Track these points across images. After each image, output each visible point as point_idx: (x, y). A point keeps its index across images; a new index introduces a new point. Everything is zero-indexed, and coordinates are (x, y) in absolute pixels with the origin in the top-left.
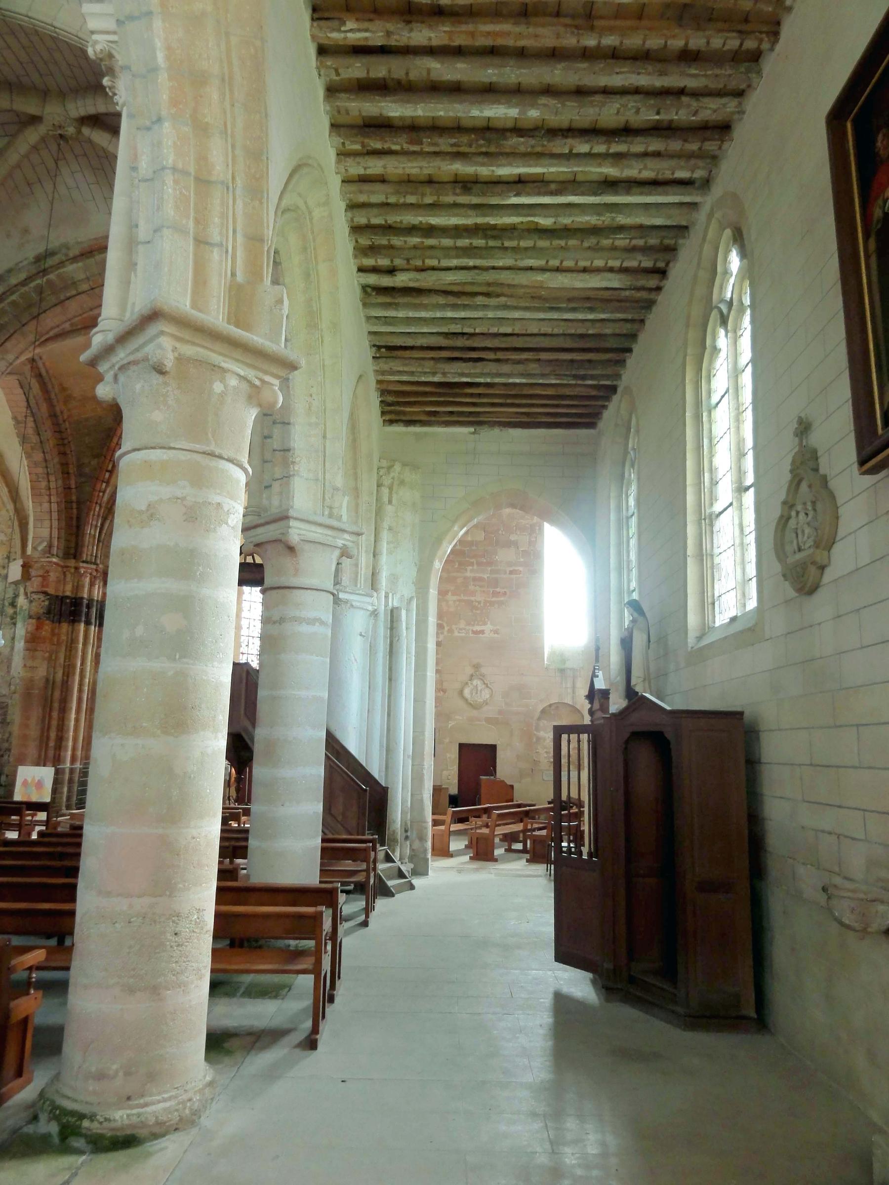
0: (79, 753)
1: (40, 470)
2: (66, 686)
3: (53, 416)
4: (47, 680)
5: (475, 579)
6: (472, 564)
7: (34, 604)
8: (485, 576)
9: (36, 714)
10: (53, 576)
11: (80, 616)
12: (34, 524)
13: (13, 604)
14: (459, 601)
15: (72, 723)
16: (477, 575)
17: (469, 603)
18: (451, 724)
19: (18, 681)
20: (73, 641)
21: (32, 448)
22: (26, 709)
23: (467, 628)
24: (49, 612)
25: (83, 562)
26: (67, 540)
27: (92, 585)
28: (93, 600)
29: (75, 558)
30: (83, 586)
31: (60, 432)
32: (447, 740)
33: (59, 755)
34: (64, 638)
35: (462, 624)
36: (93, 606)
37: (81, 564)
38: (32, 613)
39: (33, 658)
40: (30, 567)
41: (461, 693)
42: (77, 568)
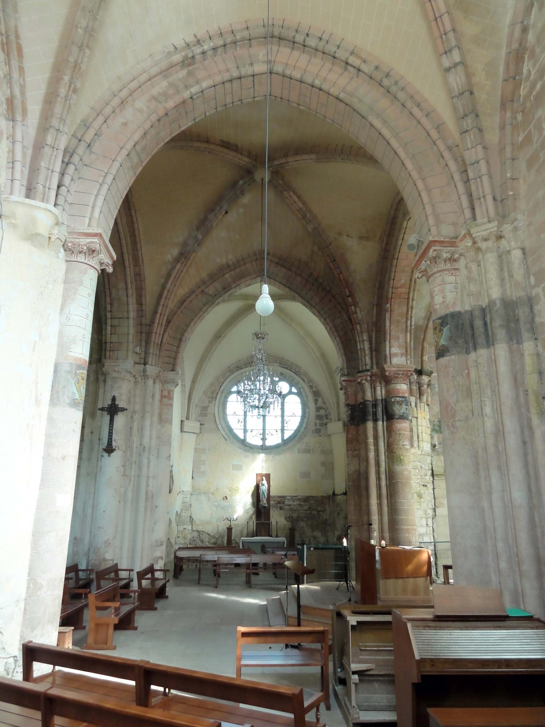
27: (374, 389)
28: (376, 400)
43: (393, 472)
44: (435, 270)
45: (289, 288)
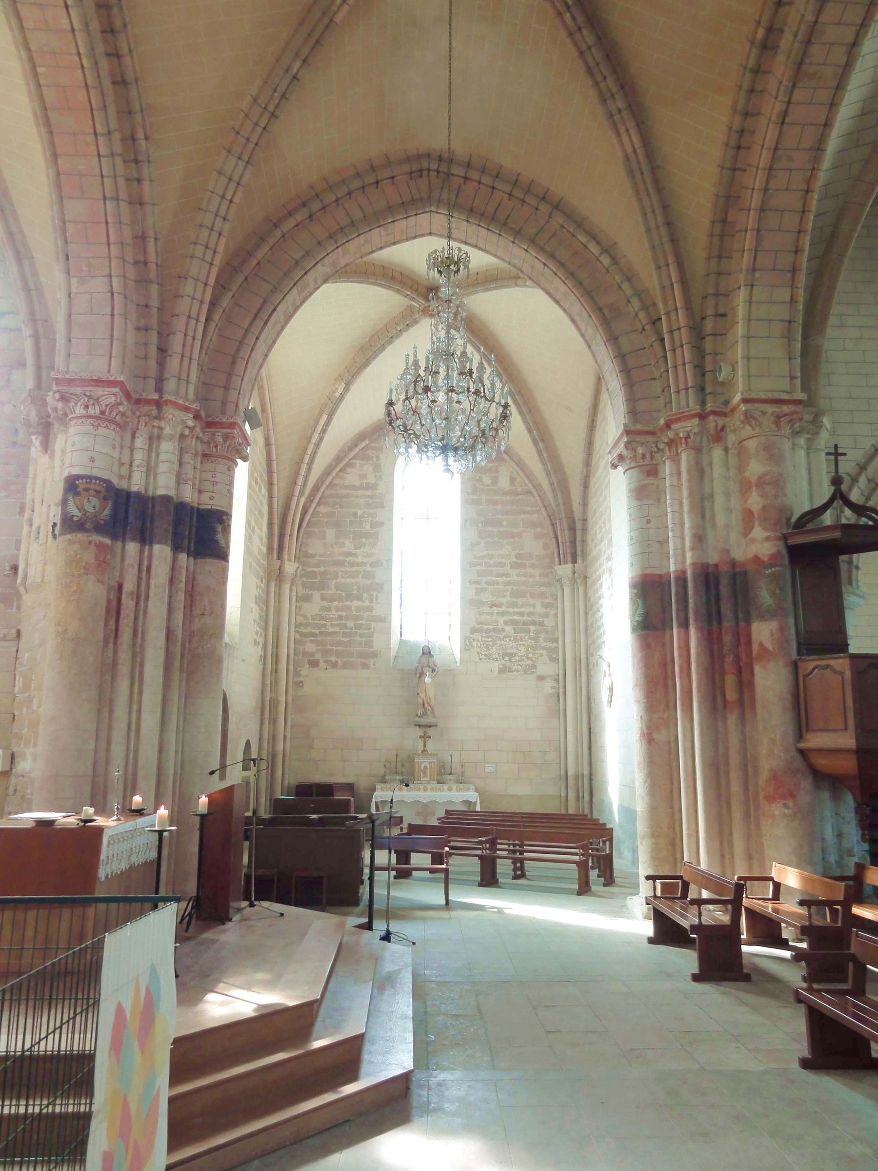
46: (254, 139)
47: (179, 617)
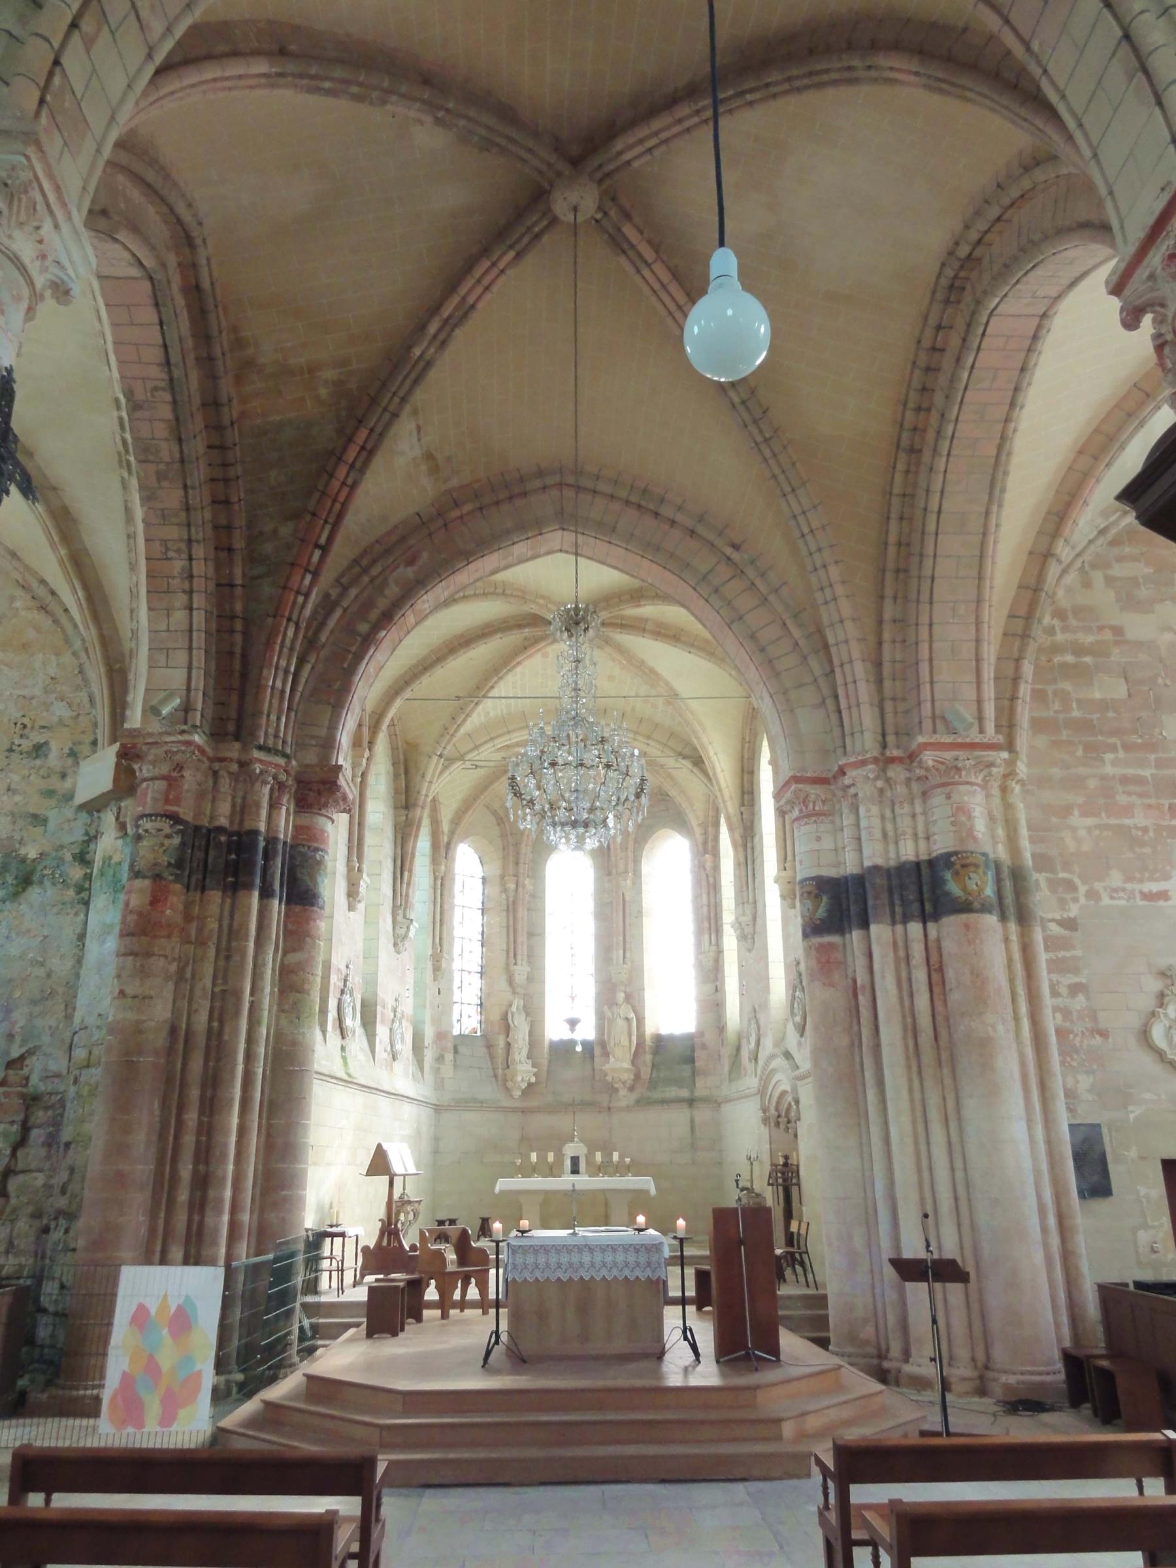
0: (245, 1218)
1: (173, 532)
2: (217, 1047)
3: (212, 404)
4: (173, 1030)
5: (1125, 780)
6: (1113, 748)
7: (145, 843)
8: (1147, 773)
9: (146, 1115)
10: (190, 780)
11: (251, 873)
12: (151, 658)
13: (83, 858)
14: (1098, 827)
15: (233, 1139)
16: (1130, 771)
17: (1120, 830)
18: (1135, 1112)
19: (97, 1035)
20: (233, 934)
21: (160, 476)
22: (122, 1102)
23: (1129, 886)
24: (179, 864)
25: (260, 748)
26: (220, 704)
27: (274, 805)
28: (276, 839)
29: (237, 737)
30: (258, 806)
31: (222, 448)
32: (1133, 1153)
33: (201, 1224)
34: (213, 925)
35: (1116, 878)
36: (275, 852)
37: (256, 754)
38: (141, 864)
39: (143, 973)
40: (139, 757)
41: (1144, 1035)
42: (244, 764)
43: (294, 1043)
44: (973, 780)
45: (171, 380)
46: (777, 471)
47: (922, 1001)
